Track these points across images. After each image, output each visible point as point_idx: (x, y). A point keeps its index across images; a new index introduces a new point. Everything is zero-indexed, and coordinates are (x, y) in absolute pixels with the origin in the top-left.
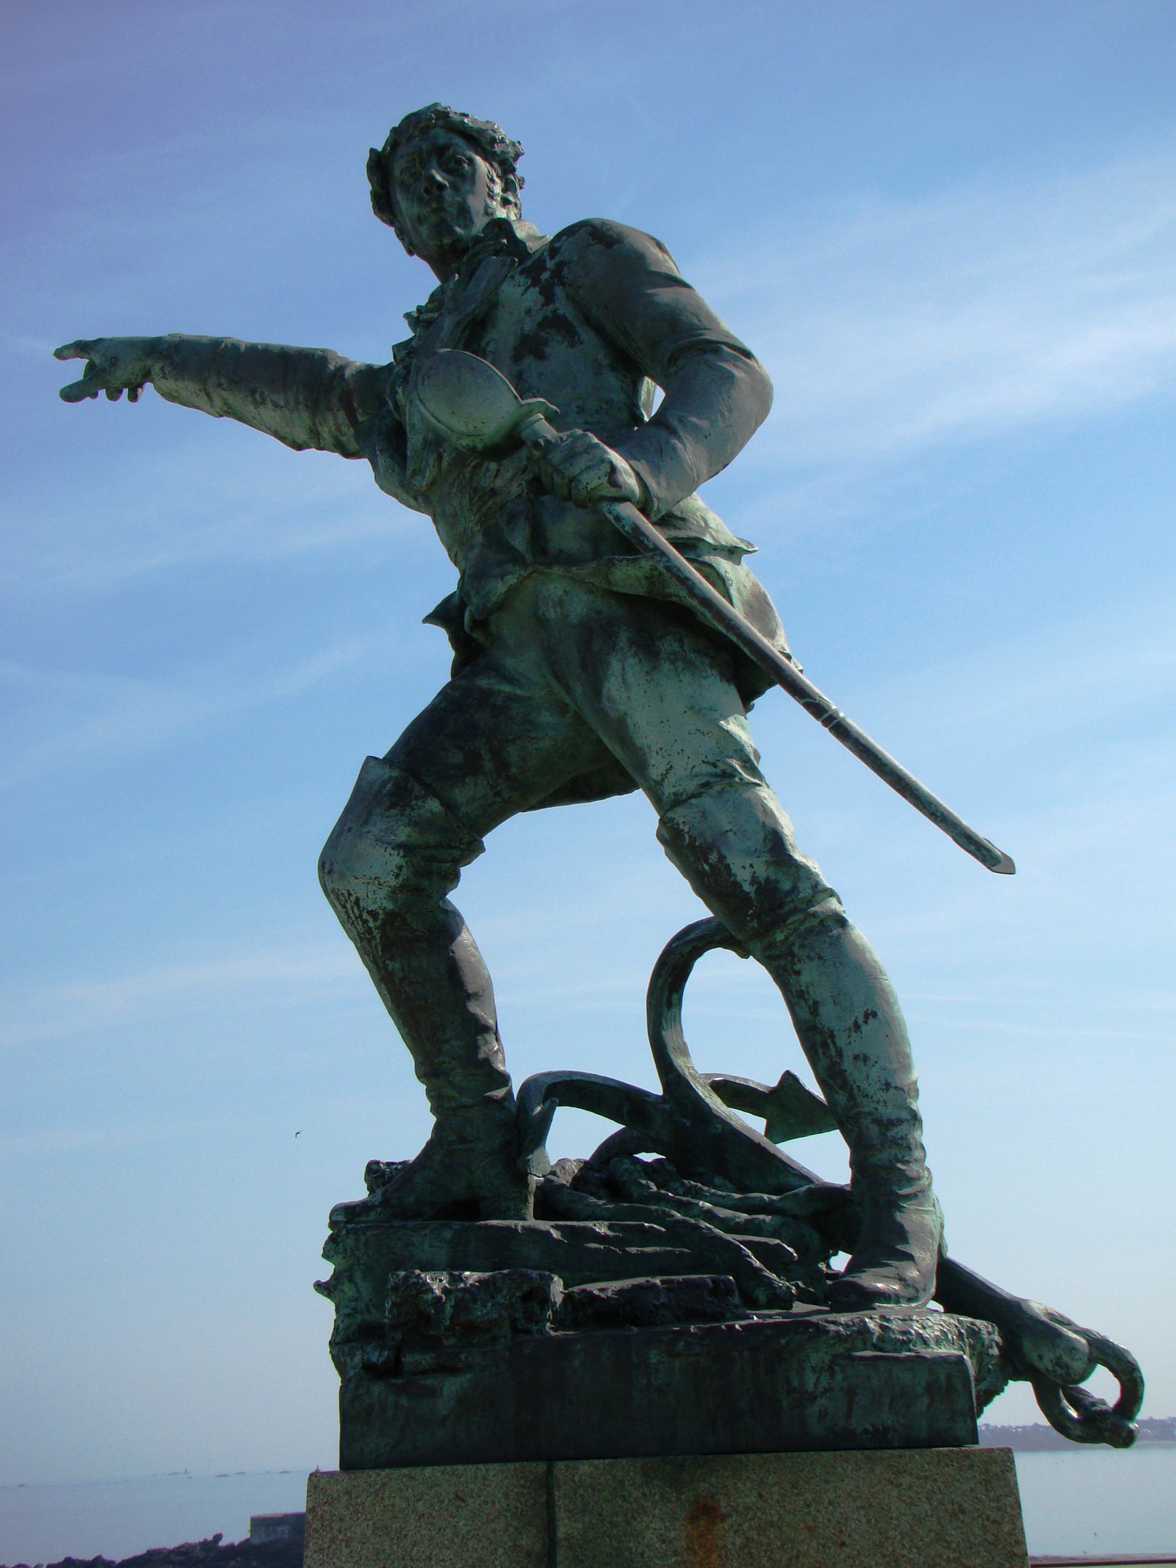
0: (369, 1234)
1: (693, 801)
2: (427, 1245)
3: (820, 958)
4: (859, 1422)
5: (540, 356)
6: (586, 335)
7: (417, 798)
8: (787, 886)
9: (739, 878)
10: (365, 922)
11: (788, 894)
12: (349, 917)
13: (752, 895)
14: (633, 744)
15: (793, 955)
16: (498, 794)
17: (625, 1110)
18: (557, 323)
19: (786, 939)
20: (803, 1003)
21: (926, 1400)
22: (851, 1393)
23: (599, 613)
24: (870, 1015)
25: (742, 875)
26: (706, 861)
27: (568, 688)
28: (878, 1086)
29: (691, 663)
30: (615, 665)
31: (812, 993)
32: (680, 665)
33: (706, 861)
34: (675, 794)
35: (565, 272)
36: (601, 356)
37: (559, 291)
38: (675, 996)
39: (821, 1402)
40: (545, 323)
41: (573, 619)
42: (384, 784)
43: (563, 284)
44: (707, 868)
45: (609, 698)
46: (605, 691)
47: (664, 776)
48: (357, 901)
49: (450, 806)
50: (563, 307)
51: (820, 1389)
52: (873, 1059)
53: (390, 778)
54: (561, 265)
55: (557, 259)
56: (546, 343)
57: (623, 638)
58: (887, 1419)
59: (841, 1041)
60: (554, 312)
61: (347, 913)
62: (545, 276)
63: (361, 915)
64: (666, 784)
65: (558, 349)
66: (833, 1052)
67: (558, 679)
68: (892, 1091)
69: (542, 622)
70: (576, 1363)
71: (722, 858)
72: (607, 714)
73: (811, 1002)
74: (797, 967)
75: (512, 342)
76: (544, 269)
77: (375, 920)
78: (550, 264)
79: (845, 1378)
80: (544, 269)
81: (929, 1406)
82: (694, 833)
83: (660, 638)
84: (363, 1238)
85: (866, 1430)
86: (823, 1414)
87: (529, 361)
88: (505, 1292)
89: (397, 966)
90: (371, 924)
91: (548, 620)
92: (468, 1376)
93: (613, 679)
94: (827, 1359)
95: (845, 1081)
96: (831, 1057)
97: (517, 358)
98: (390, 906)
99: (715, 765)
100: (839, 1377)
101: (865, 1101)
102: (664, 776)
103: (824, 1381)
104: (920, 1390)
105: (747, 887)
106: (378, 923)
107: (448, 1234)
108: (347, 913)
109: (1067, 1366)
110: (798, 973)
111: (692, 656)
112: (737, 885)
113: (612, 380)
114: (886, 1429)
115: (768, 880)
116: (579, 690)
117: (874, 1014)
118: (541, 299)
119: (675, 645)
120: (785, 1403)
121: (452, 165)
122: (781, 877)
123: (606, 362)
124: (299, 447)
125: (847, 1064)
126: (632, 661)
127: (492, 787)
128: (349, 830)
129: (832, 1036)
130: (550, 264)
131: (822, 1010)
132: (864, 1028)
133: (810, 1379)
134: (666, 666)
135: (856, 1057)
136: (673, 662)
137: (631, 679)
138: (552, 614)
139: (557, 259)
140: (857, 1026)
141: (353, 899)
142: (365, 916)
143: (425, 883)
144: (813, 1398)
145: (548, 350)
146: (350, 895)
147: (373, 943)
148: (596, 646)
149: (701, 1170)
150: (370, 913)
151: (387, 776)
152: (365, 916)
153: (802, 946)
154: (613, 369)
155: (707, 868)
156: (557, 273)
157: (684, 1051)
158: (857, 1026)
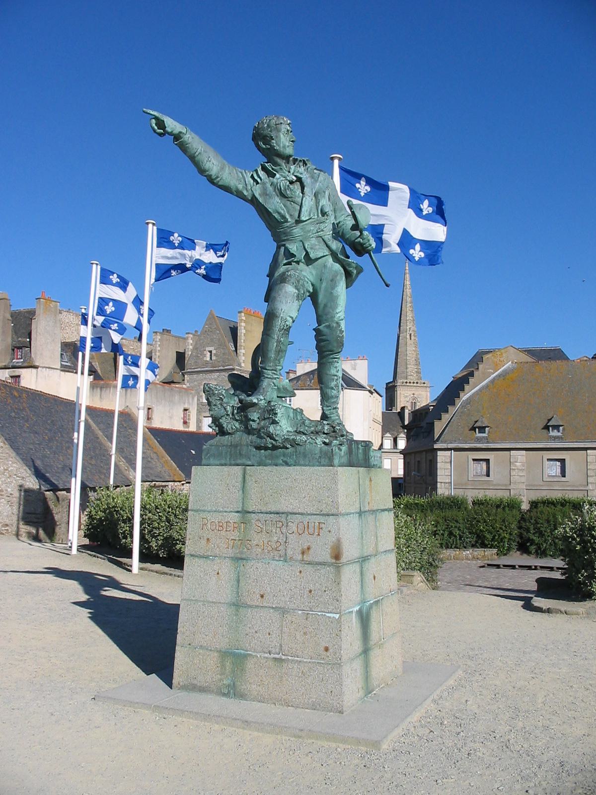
14: (336, 303)
34: (339, 317)
41: (334, 269)
46: (336, 289)
48: (285, 322)
93: (340, 287)
142: (285, 326)
148: (338, 278)
152: (285, 326)
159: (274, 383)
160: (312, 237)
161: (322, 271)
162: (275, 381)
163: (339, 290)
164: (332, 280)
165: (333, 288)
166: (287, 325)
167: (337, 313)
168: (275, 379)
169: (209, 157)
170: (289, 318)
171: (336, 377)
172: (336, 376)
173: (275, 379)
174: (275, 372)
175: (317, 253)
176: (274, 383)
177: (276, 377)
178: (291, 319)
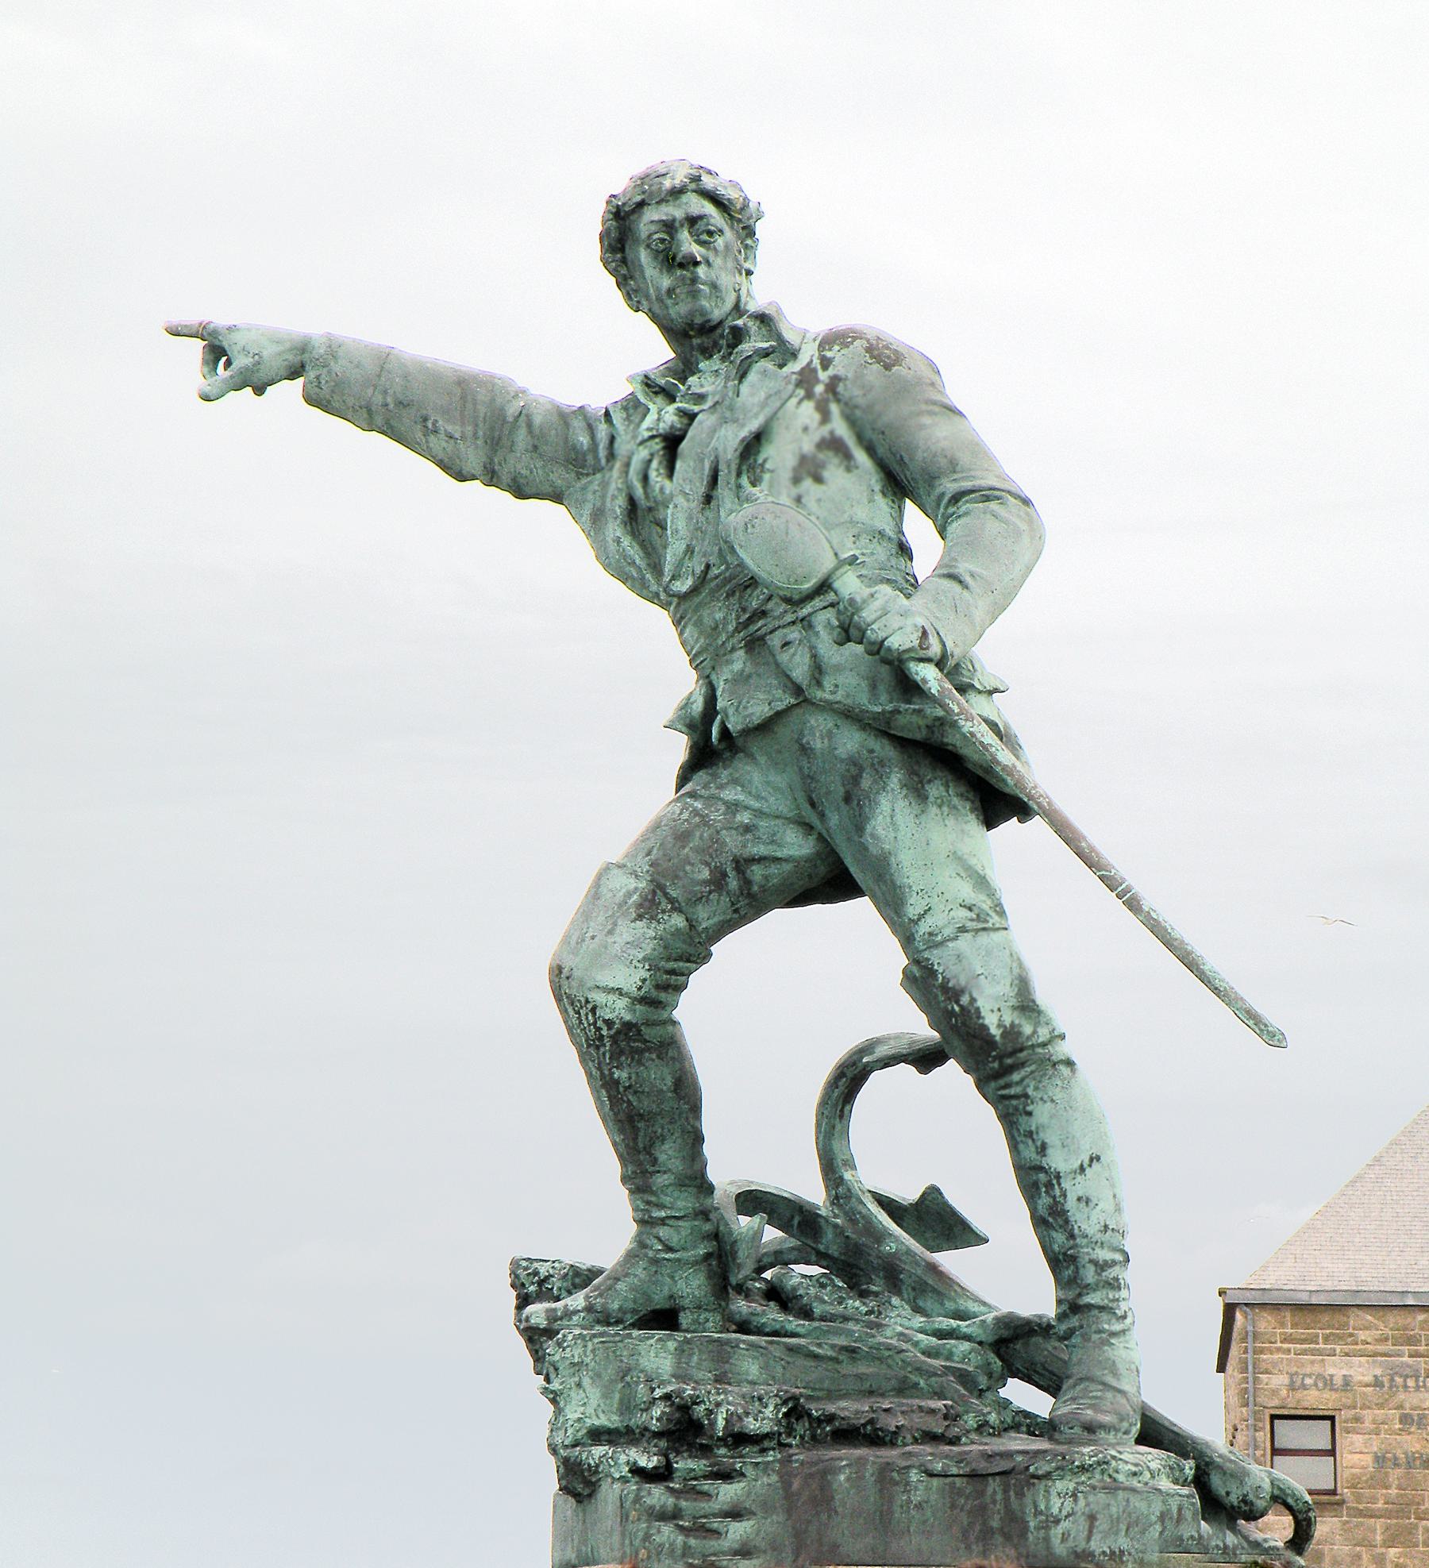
0: (596, 1340)
1: (950, 944)
2: (652, 1354)
3: (1052, 1101)
4: (1097, 1545)
5: (818, 479)
6: (861, 456)
7: (664, 912)
8: (1027, 1029)
9: (987, 1022)
10: (599, 1029)
11: (1029, 1038)
12: (581, 1022)
13: (998, 1038)
14: (893, 882)
15: (1026, 1096)
16: (736, 911)
17: (796, 1222)
18: (834, 444)
19: (1022, 1080)
20: (1030, 1142)
21: (1158, 1527)
22: (1092, 1518)
23: (871, 751)
24: (1094, 1159)
25: (991, 1021)
26: (957, 1002)
27: (822, 816)
28: (1098, 1227)
29: (955, 807)
30: (885, 803)
31: (1041, 1135)
32: (945, 809)
33: (957, 1002)
34: (930, 934)
35: (840, 388)
36: (873, 481)
37: (834, 408)
38: (848, 1107)
39: (1064, 1525)
40: (823, 444)
42: (629, 894)
43: (838, 401)
44: (957, 1008)
45: (872, 836)
46: (869, 829)
47: (921, 916)
48: (594, 1010)
49: (692, 924)
50: (839, 427)
51: (1064, 1513)
52: (1095, 1201)
53: (636, 889)
54: (835, 380)
55: (831, 372)
56: (822, 465)
57: (895, 779)
58: (1123, 1543)
59: (1066, 1184)
60: (832, 433)
61: (579, 1018)
62: (819, 389)
63: (595, 1023)
64: (921, 923)
65: (834, 473)
66: (1057, 1192)
67: (813, 805)
68: (1109, 1232)
69: (805, 750)
70: (842, 1477)
71: (973, 1000)
72: (866, 849)
73: (1039, 1143)
74: (1029, 1108)
75: (791, 461)
76: (817, 381)
77: (609, 1029)
78: (823, 376)
79: (1087, 1505)
80: (817, 381)
81: (1161, 1533)
82: (948, 974)
83: (929, 781)
84: (590, 1344)
85: (1104, 1553)
86: (1065, 1537)
87: (808, 483)
88: (771, 1408)
89: (624, 1075)
90: (604, 1032)
91: (812, 749)
92: (742, 1485)
94: (1071, 1486)
95: (1067, 1221)
96: (1054, 1198)
97: (796, 480)
98: (628, 1017)
99: (970, 909)
100: (1082, 1502)
101: (1085, 1241)
102: (921, 916)
103: (1069, 1504)
104: (1154, 1518)
105: (995, 1031)
106: (612, 1032)
107: (671, 1345)
108: (579, 1018)
109: (1252, 1504)
110: (1030, 1114)
111: (956, 801)
112: (985, 1028)
113: (883, 504)
114: (1122, 1552)
115: (1012, 1025)
116: (834, 820)
117: (1098, 1158)
118: (817, 417)
119: (942, 788)
120: (1032, 1524)
121: (705, 237)
122: (1024, 1022)
123: (877, 488)
124: (461, 477)
125: (1071, 1204)
126: (901, 804)
127: (733, 904)
128: (593, 938)
129: (1058, 1177)
130: (823, 376)
131: (1050, 1151)
132: (1088, 1170)
133: (1056, 1504)
134: (934, 810)
135: (1079, 1199)
136: (940, 806)
137: (899, 818)
138: (818, 744)
139: (831, 372)
140: (1082, 1169)
141: (590, 1006)
143: (663, 996)
144: (1057, 1522)
145: (826, 474)
146: (587, 1001)
147: (602, 1050)
148: (866, 783)
149: (874, 1288)
150: (605, 1021)
151: (632, 887)
153: (1036, 1088)
154: (884, 495)
155: (957, 1008)
156: (832, 386)
157: (850, 1164)
158: (1082, 1169)
159: (659, 1239)
160: (733, 650)
161: (801, 769)
162: (663, 1232)
163: (880, 831)
164: (847, 799)
165: (860, 829)
166: (609, 1023)
167: (916, 922)
168: (663, 1221)
169: (425, 420)
170: (599, 998)
171: (1042, 1177)
172: (1041, 1169)
173: (663, 1221)
174: (653, 1199)
175: (750, 711)
176: (659, 1239)
177: (663, 1214)
178: (611, 997)
